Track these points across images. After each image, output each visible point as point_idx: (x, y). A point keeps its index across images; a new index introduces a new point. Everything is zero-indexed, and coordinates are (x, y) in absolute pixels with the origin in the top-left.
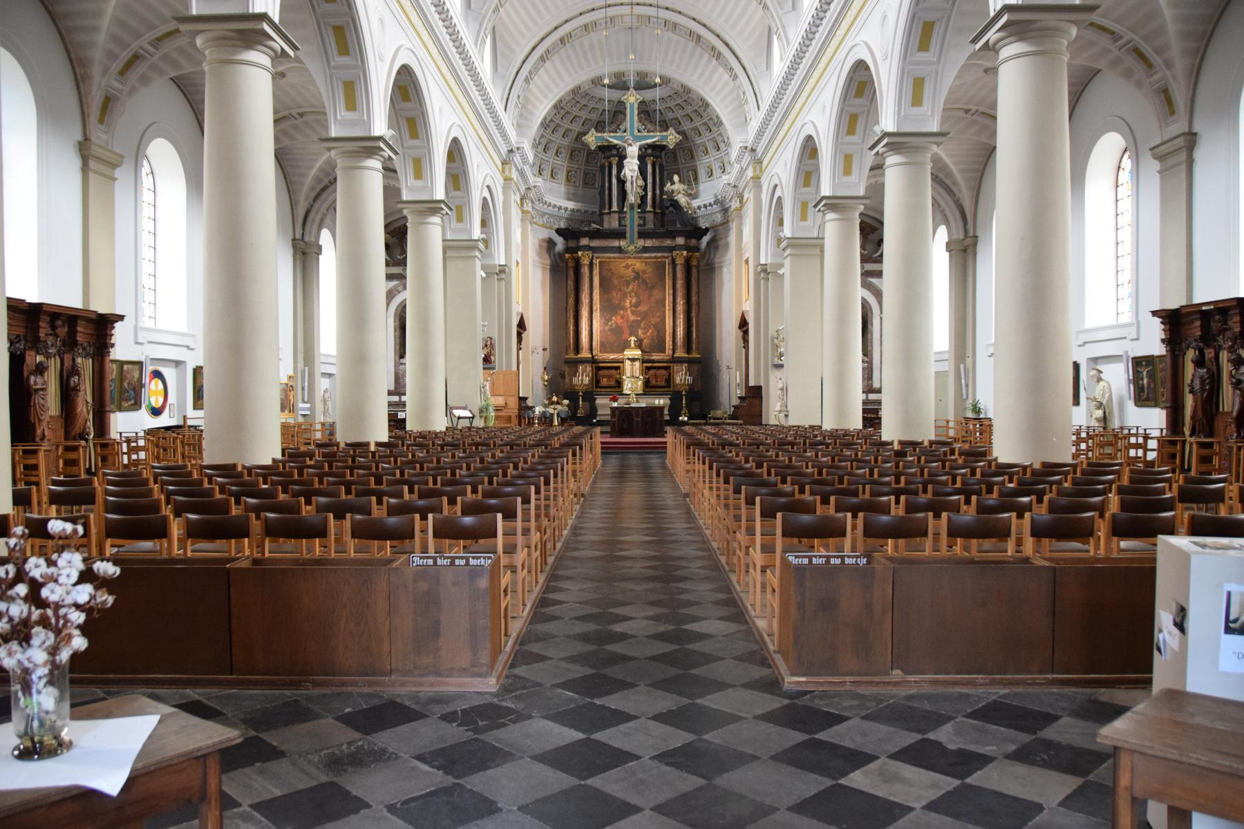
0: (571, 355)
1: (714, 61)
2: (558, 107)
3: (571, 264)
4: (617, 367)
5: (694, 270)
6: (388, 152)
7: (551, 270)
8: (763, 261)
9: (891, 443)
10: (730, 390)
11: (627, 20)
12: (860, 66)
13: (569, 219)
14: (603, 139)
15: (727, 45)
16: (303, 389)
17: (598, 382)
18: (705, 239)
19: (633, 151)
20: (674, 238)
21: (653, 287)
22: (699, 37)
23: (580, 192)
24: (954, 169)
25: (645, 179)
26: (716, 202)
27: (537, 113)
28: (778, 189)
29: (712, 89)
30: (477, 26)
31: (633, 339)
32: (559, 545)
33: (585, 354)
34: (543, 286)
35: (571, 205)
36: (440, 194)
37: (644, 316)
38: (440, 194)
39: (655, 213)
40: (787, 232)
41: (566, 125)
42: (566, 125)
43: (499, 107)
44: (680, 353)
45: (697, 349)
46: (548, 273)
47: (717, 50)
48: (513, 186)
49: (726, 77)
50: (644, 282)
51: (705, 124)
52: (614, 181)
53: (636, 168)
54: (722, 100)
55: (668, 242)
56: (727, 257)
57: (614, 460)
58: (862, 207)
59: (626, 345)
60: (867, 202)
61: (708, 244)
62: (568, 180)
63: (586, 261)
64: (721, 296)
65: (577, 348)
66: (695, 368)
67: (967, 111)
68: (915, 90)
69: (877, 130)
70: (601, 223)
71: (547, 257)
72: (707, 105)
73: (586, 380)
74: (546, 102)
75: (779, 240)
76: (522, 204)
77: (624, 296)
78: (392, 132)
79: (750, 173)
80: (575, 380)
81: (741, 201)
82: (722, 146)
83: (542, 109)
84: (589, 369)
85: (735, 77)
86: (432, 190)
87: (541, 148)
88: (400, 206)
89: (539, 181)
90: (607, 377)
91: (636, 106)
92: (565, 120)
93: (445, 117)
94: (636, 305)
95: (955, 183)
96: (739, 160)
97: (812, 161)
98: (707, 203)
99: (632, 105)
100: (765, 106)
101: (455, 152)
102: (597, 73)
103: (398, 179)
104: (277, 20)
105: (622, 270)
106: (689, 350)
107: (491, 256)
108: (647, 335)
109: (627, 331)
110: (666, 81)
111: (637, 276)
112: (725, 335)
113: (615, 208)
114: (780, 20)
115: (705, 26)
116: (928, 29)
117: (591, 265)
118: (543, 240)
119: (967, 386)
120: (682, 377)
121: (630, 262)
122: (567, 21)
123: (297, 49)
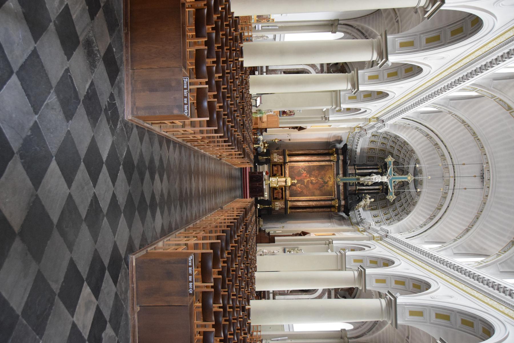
0: (287, 153)
1: (428, 217)
2: (405, 143)
3: (330, 151)
4: (282, 174)
5: (329, 210)
6: (381, 63)
8: (334, 242)
9: (249, 305)
10: (272, 228)
11: (447, 175)
12: (428, 286)
13: (351, 150)
14: (390, 165)
15: (436, 223)
16: (268, 26)
17: (275, 165)
18: (344, 215)
19: (385, 179)
20: (344, 199)
21: (321, 190)
22: (440, 209)
23: (365, 155)
24: (380, 332)
25: (371, 185)
26: (362, 219)
28: (369, 249)
30: (442, 104)
31: (296, 181)
32: (196, 148)
33: (288, 159)
34: (319, 138)
35: (358, 150)
36: (362, 88)
37: (307, 187)
38: (362, 88)
39: (356, 190)
40: (348, 253)
41: (397, 147)
42: (397, 147)
43: (404, 115)
44: (289, 204)
45: (292, 212)
46: (326, 141)
47: (434, 218)
48: (367, 123)
49: (421, 223)
50: (323, 186)
51: (399, 213)
52: (370, 171)
53: (377, 181)
54: (410, 221)
55: (342, 197)
56: (336, 225)
57: (238, 174)
58: (361, 288)
59: (292, 178)
60: (364, 291)
61: (342, 216)
62: (371, 149)
63: (332, 158)
64: (317, 222)
65: (290, 155)
66: (283, 211)
67: (408, 337)
68: (417, 312)
69: (398, 295)
70: (350, 165)
71: (334, 140)
72: (408, 214)
73: (275, 160)
74: (407, 137)
75: (344, 250)
76: (358, 127)
77: (316, 177)
78: (390, 64)
79: (376, 235)
80: (275, 155)
81: (362, 231)
82: (388, 221)
83: (404, 136)
84: (281, 161)
85: (421, 227)
86: (363, 84)
87: (385, 136)
88: (355, 69)
89: (369, 135)
90: (278, 170)
91: (406, 180)
92: (398, 147)
93: (398, 90)
94: (312, 183)
95: (373, 333)
96: (382, 229)
97: (382, 264)
98: (361, 215)
99: (406, 178)
100: (408, 241)
101: (382, 95)
102: (421, 161)
103: (368, 68)
104: (442, 8)
105: (328, 176)
106: (291, 208)
107: (333, 113)
108: (298, 188)
109: (299, 178)
110: (419, 194)
111: (326, 183)
112: (299, 225)
113: (357, 171)
114: (449, 248)
115: (445, 212)
116: (447, 318)
117: (330, 161)
118: (341, 138)
119: (278, 340)
120: (278, 205)
121: (332, 179)
122: (446, 146)
123: (428, 18)
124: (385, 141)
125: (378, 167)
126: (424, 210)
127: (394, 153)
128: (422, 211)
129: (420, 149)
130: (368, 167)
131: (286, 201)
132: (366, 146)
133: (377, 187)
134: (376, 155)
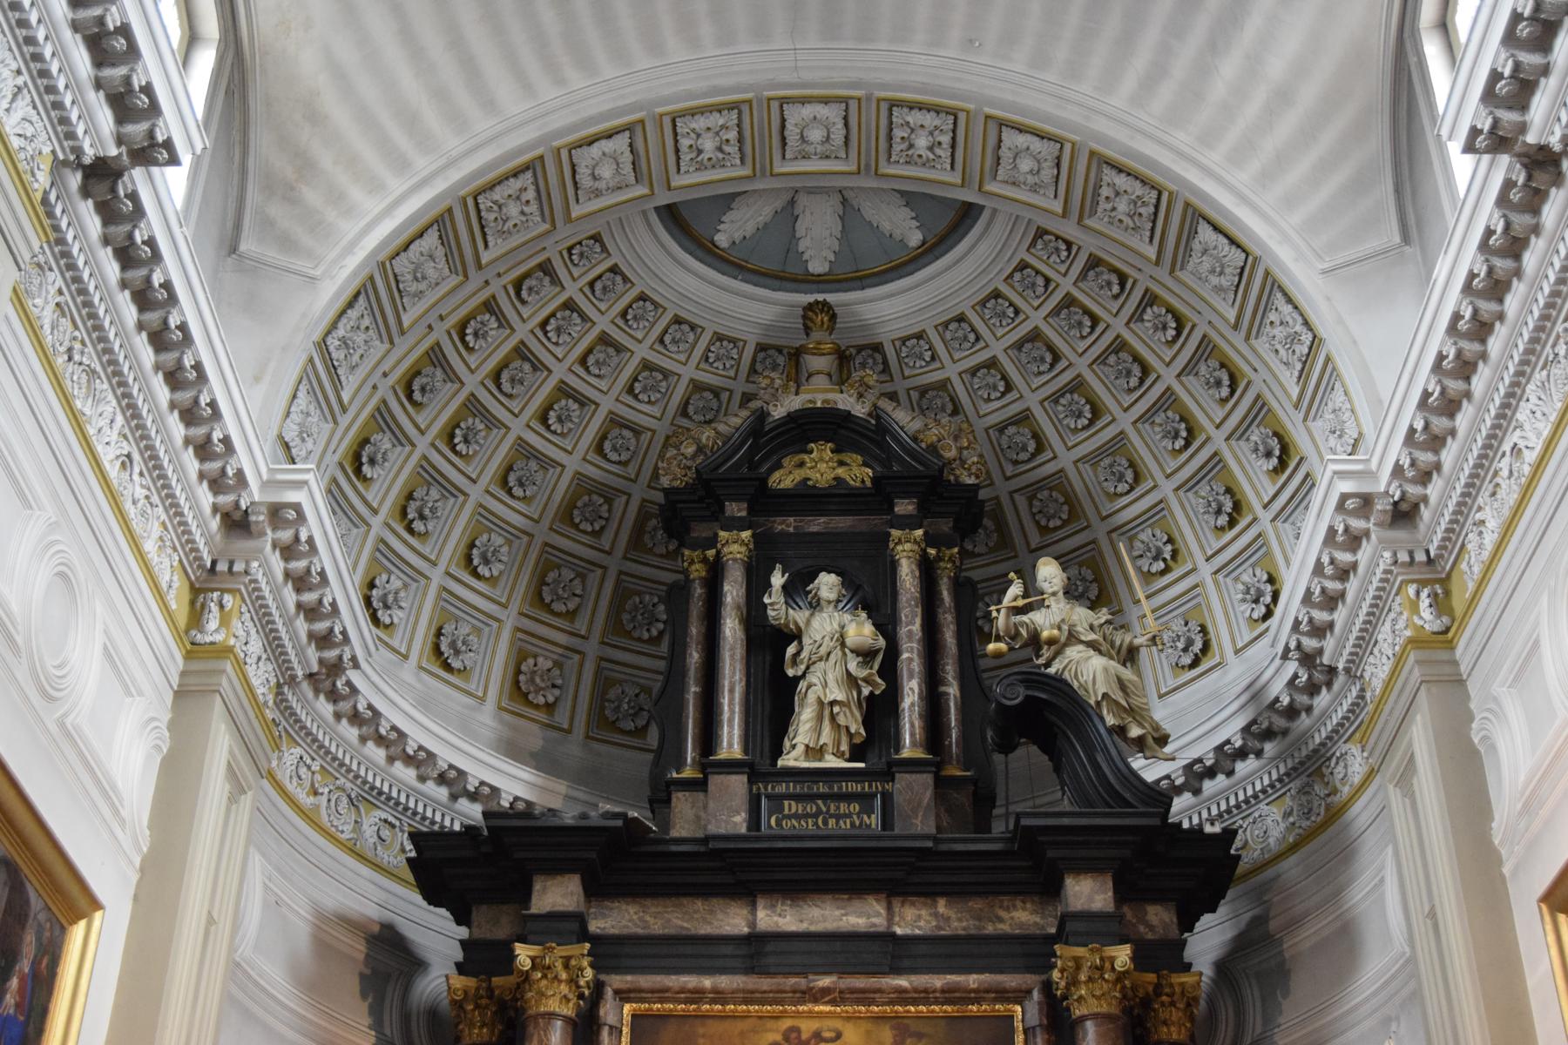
18: (1208, 941)
20: (1051, 890)
23: (574, 748)
25: (886, 625)
26: (1258, 734)
29: (1208, 138)
39: (941, 783)
52: (731, 628)
54: (1266, 177)
55: (1022, 917)
61: (1223, 967)
62: (518, 691)
74: (397, 186)
76: (197, 616)
81: (1441, 604)
83: (367, 217)
113: (731, 743)
125: (698, 571)
126: (1140, 62)
127: (573, 464)
128: (1157, 73)
129: (527, 87)
130: (695, 657)
132: (487, 718)
133: (907, 574)
134: (592, 648)
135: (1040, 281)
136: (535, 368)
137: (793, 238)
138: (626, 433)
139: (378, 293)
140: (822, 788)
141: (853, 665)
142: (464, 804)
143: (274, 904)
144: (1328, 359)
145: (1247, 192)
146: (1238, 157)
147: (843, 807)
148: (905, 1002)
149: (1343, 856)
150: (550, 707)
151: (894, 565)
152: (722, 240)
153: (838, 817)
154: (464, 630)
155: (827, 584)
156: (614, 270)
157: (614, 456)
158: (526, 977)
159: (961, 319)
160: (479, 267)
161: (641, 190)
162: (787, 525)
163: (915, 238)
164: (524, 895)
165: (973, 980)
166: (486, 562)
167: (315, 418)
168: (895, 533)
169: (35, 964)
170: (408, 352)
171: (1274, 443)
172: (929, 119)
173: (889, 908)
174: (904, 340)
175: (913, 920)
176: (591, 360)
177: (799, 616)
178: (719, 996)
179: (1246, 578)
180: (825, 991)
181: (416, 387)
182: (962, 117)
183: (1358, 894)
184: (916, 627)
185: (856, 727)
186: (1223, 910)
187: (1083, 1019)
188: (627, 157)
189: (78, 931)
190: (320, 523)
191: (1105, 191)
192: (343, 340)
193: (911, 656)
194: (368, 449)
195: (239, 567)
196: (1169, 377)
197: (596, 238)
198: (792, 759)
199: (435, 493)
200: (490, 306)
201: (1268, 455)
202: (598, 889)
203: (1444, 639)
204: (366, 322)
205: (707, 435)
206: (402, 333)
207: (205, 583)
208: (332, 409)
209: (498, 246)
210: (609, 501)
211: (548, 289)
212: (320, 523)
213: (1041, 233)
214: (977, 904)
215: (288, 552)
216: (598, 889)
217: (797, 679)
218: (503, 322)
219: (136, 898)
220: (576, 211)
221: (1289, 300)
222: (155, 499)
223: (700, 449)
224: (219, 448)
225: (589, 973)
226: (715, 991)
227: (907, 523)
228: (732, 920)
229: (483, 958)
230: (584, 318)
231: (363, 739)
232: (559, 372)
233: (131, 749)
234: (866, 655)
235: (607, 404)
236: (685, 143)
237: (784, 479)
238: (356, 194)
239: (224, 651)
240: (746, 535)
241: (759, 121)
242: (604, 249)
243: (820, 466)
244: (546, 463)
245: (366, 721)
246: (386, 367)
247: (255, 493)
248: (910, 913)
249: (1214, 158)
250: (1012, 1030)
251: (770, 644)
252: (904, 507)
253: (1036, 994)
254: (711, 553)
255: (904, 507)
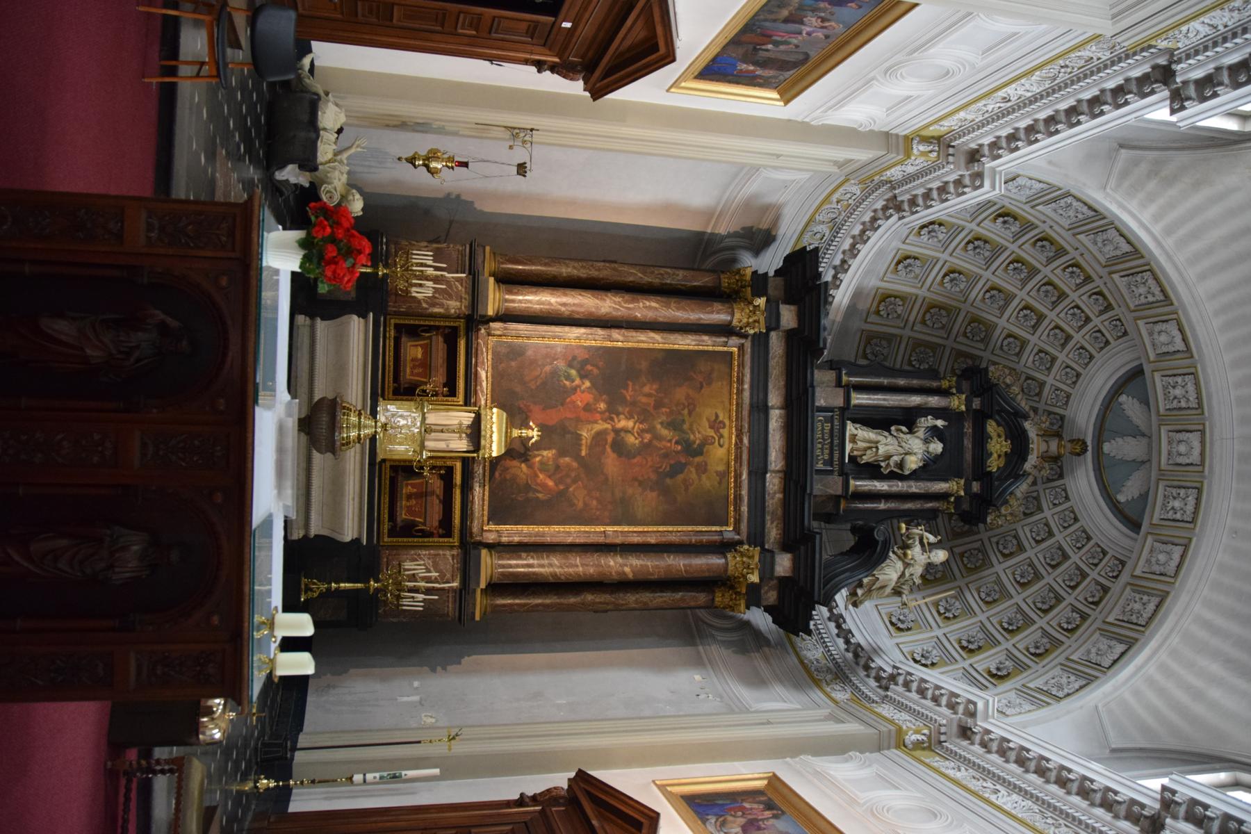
4: (455, 386)
5: (702, 598)
7: (699, 236)
18: (760, 618)
20: (786, 547)
21: (665, 492)
23: (857, 324)
26: (857, 650)
27: (1133, 205)
29: (1174, 653)
31: (534, 434)
33: (494, 299)
34: (668, 208)
37: (591, 468)
39: (837, 499)
44: (490, 566)
45: (497, 610)
46: (696, 227)
50: (677, 469)
52: (916, 400)
54: (1151, 682)
55: (773, 533)
59: (516, 416)
61: (747, 625)
62: (886, 297)
63: (739, 317)
64: (631, 664)
65: (509, 281)
66: (451, 608)
73: (423, 292)
74: (1157, 229)
76: (926, 140)
77: (644, 415)
81: (918, 745)
83: (1139, 215)
84: (454, 306)
90: (428, 354)
94: (619, 446)
105: (708, 412)
106: (498, 587)
108: (540, 474)
109: (553, 417)
111: (694, 450)
112: (533, 681)
113: (859, 399)
117: (725, 330)
121: (729, 434)
124: (968, 262)
126: (1220, 621)
127: (1002, 322)
130: (901, 382)
131: (470, 548)
132: (873, 282)
133: (941, 487)
134: (907, 332)
135: (1096, 561)
136: (1053, 303)
137: (1123, 435)
138: (1017, 350)
139: (1097, 222)
140: (836, 442)
141: (896, 458)
142: (832, 272)
143: (786, 185)
144: (1048, 704)
145: (1144, 671)
146: (1163, 668)
147: (827, 451)
148: (736, 477)
149: (797, 685)
150: (878, 312)
151: (946, 480)
152: (1123, 398)
153: (822, 449)
154: (917, 271)
155: (937, 447)
156: (1107, 343)
157: (1005, 343)
158: (751, 303)
159: (1076, 520)
160: (1110, 273)
161: (1152, 357)
162: (968, 428)
163: (1121, 498)
164: (787, 302)
165: (745, 509)
166: (952, 280)
167: (1028, 192)
168: (962, 482)
169: (760, 77)
170: (1063, 238)
171: (1004, 673)
172: (1190, 508)
173: (779, 471)
174: (1065, 490)
175: (773, 482)
176: (1057, 331)
177: (921, 433)
178: (740, 392)
179: (935, 652)
180: (741, 440)
181: (1044, 243)
182: (1191, 526)
183: (779, 690)
184: (914, 490)
185: (865, 459)
186: (774, 627)
187: (726, 558)
188: (1171, 349)
189: (775, 95)
190: (973, 197)
191: (1145, 598)
192: (1071, 205)
193: (899, 486)
194: (1011, 220)
195: (951, 159)
196: (1041, 623)
197: (1125, 333)
198: (850, 428)
199: (987, 254)
200: (1088, 279)
201: (998, 669)
202: (790, 335)
203: (901, 744)
204: (1080, 216)
205: (1016, 389)
206: (1074, 235)
207: (942, 143)
208: (1033, 201)
209: (1121, 282)
210: (982, 341)
211: (1097, 309)
212: (973, 197)
213: (1123, 563)
214: (780, 512)
215: (958, 183)
216: (790, 335)
217: (889, 431)
218: (1079, 286)
219: (789, 120)
220: (1141, 323)
221: (1081, 687)
222: (987, 115)
223: (1008, 386)
224: (1013, 146)
225: (752, 332)
226: (743, 390)
227: (967, 488)
228: (775, 398)
229: (759, 283)
230: (1081, 328)
231: (863, 224)
232: (1052, 315)
233: (862, 112)
234: (901, 465)
235: (1033, 339)
236: (1179, 379)
237: (992, 427)
238: (1153, 208)
239: (908, 154)
240: (963, 408)
241: (1192, 418)
242: (1120, 337)
243: (998, 446)
244: (1003, 309)
245: (873, 225)
246: (1056, 227)
247: (989, 164)
248: (776, 481)
249: (1163, 656)
250: (721, 525)
251: (908, 419)
252: (976, 487)
253: (737, 537)
254: (954, 391)
255: (976, 487)
